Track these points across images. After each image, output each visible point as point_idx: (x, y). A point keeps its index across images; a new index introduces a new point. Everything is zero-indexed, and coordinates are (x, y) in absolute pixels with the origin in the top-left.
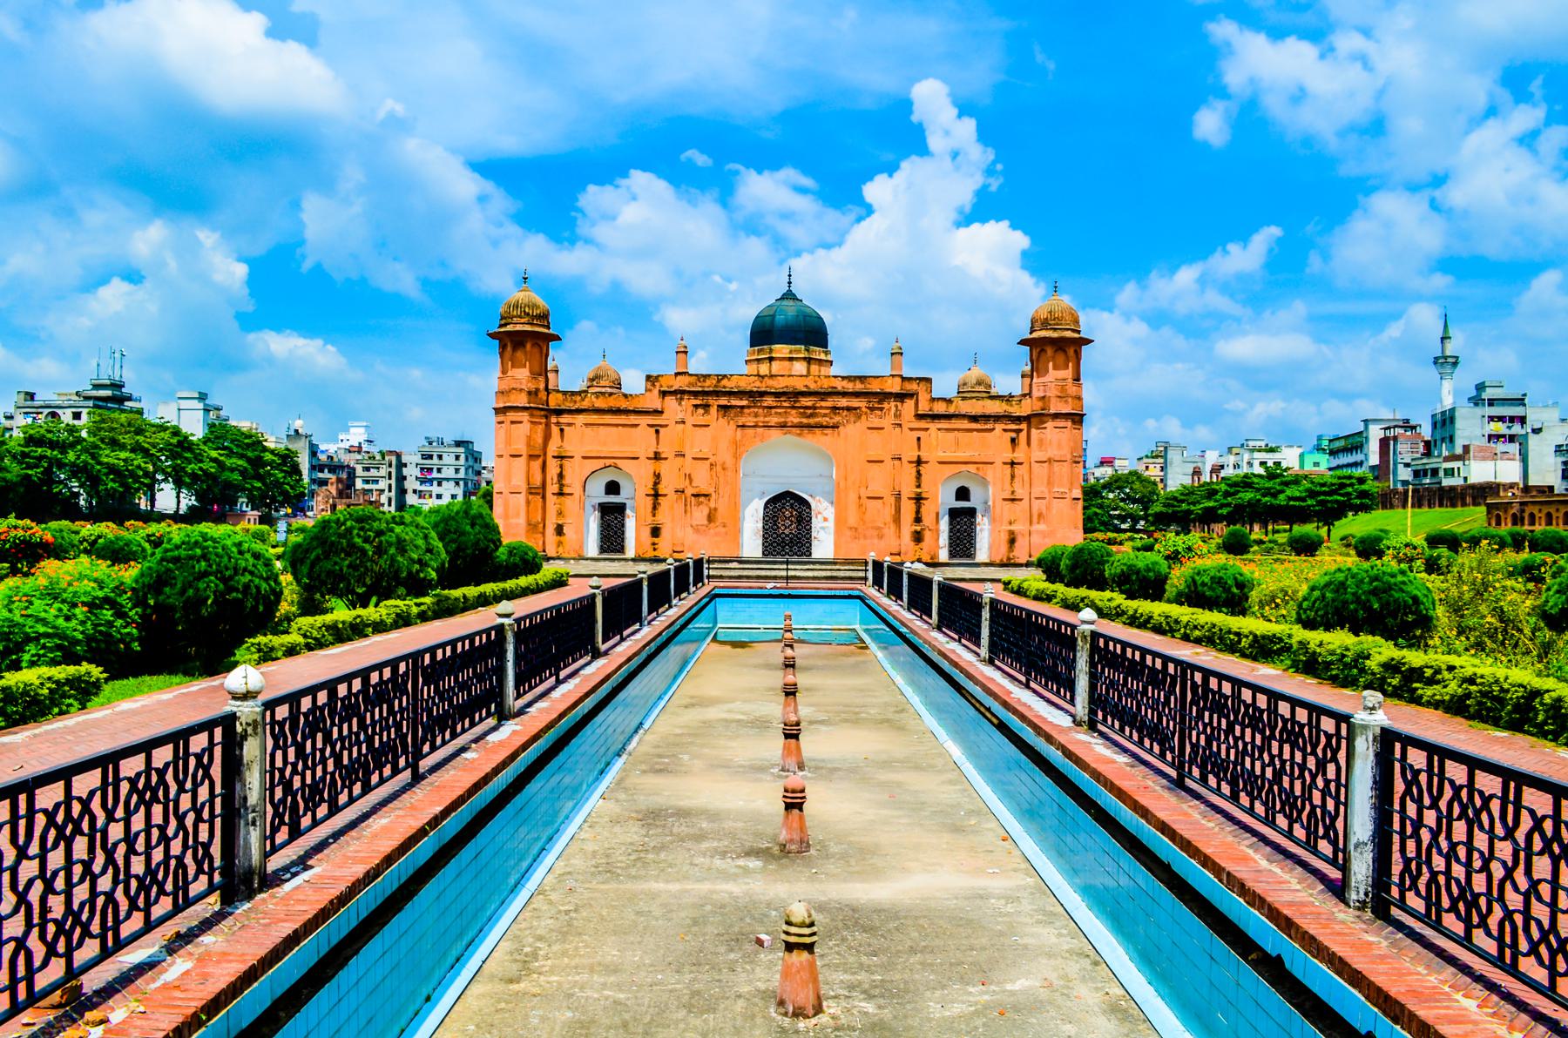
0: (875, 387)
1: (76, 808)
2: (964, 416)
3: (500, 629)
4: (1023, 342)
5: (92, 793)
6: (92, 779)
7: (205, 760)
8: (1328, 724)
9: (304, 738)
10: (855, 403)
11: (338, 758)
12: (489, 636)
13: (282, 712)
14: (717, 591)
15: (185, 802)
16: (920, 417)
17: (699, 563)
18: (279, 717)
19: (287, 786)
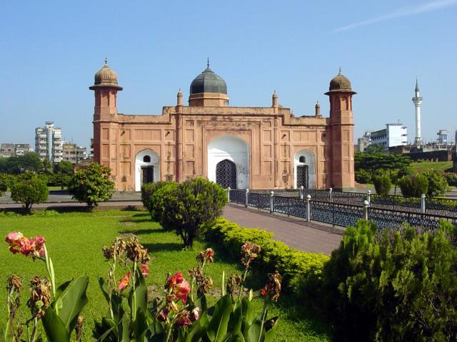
2: (304, 125)
10: (258, 119)
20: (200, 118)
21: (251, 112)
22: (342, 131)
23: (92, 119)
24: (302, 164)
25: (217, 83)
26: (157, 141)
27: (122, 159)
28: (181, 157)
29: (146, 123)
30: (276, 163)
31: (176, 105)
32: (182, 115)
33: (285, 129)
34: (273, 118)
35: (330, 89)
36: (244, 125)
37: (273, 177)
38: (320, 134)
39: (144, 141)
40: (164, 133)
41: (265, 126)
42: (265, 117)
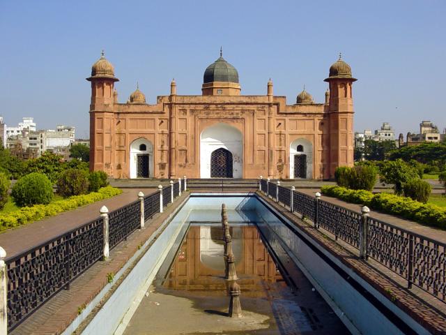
0: (260, 100)
2: (300, 114)
4: (326, 80)
10: (252, 107)
14: (192, 194)
16: (278, 113)
20: (192, 107)
21: (245, 100)
22: (340, 119)
24: (299, 153)
25: (229, 71)
26: (151, 130)
27: (117, 148)
28: (173, 146)
29: (141, 113)
30: (271, 152)
32: (175, 104)
34: (267, 106)
35: (330, 76)
36: (237, 114)
37: (266, 166)
38: (318, 122)
39: (139, 130)
40: (158, 122)
41: (259, 114)
42: (259, 106)
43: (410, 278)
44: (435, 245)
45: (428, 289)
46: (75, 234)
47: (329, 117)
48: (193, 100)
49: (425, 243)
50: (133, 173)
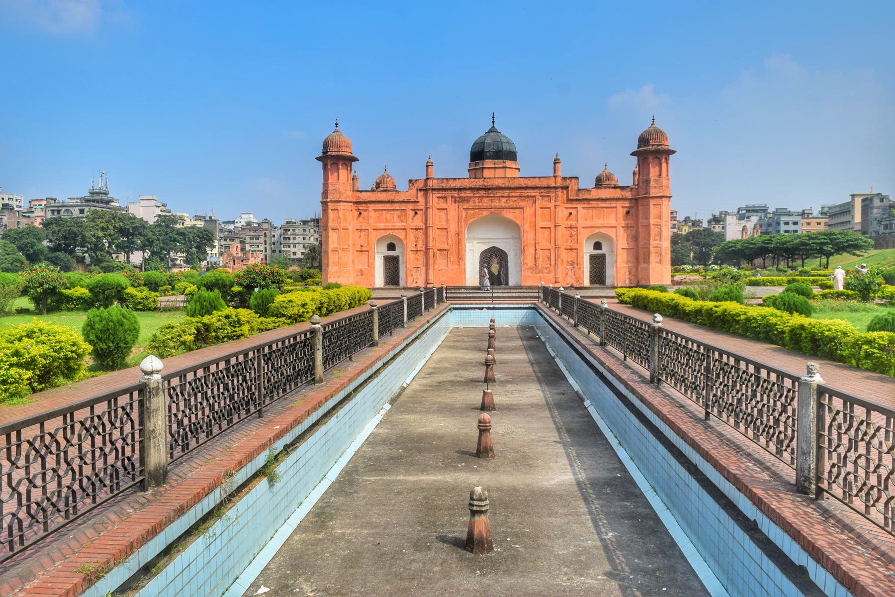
1: (48, 439)
3: (313, 332)
4: (633, 154)
5: (57, 430)
6: (58, 422)
7: (128, 410)
8: (788, 383)
9: (189, 395)
10: (532, 193)
11: (211, 407)
12: (305, 335)
13: (175, 382)
15: (116, 434)
16: (569, 200)
17: (440, 290)
18: (172, 384)
19: (180, 423)
21: (523, 183)
23: (320, 198)
25: (506, 147)
28: (431, 244)
31: (425, 177)
32: (433, 190)
33: (570, 206)
37: (552, 268)
38: (622, 212)
41: (540, 202)
43: (707, 406)
44: (778, 377)
45: (728, 420)
46: (270, 347)
47: (637, 203)
48: (458, 184)
49: (743, 365)
50: (379, 280)
